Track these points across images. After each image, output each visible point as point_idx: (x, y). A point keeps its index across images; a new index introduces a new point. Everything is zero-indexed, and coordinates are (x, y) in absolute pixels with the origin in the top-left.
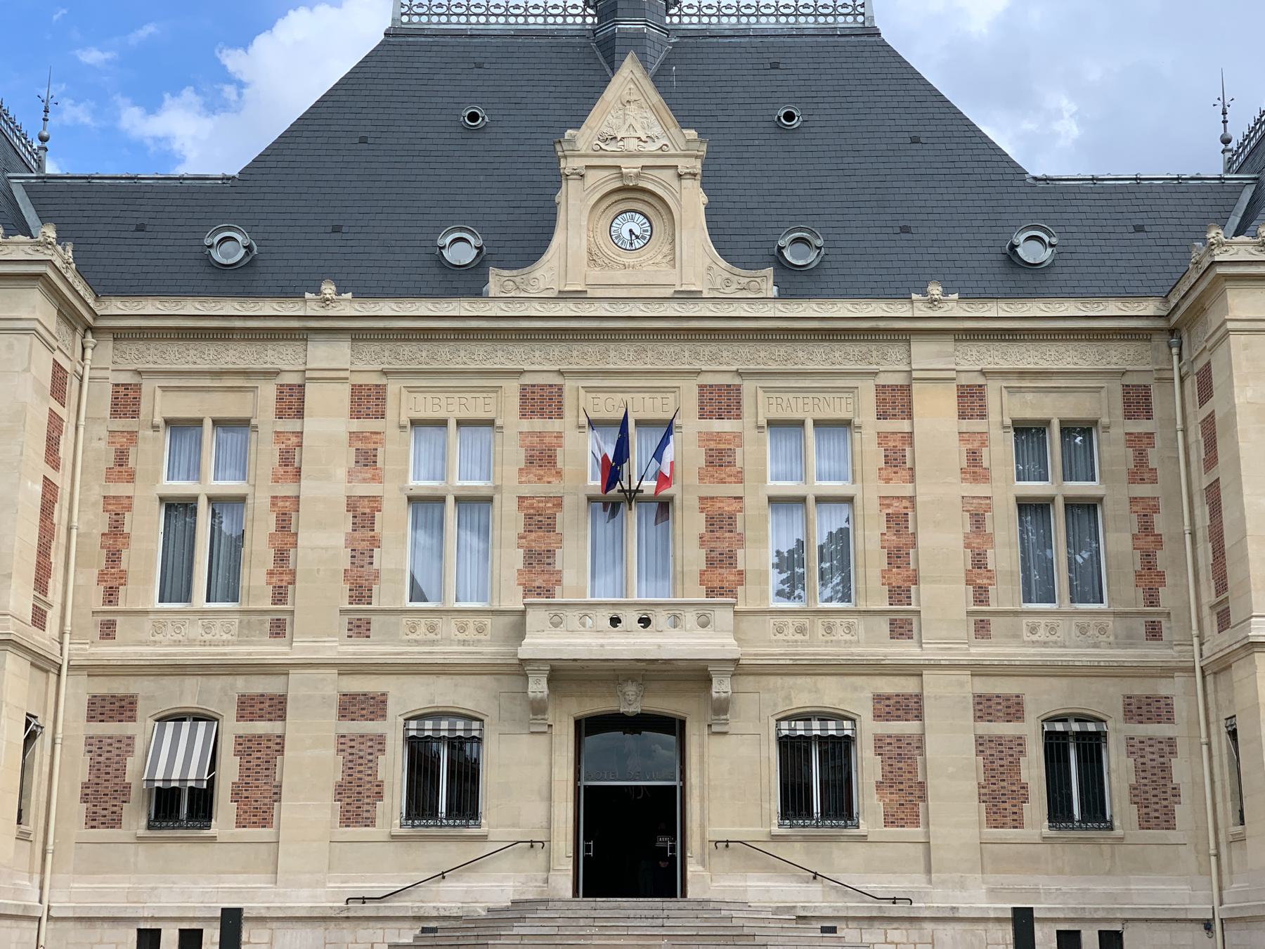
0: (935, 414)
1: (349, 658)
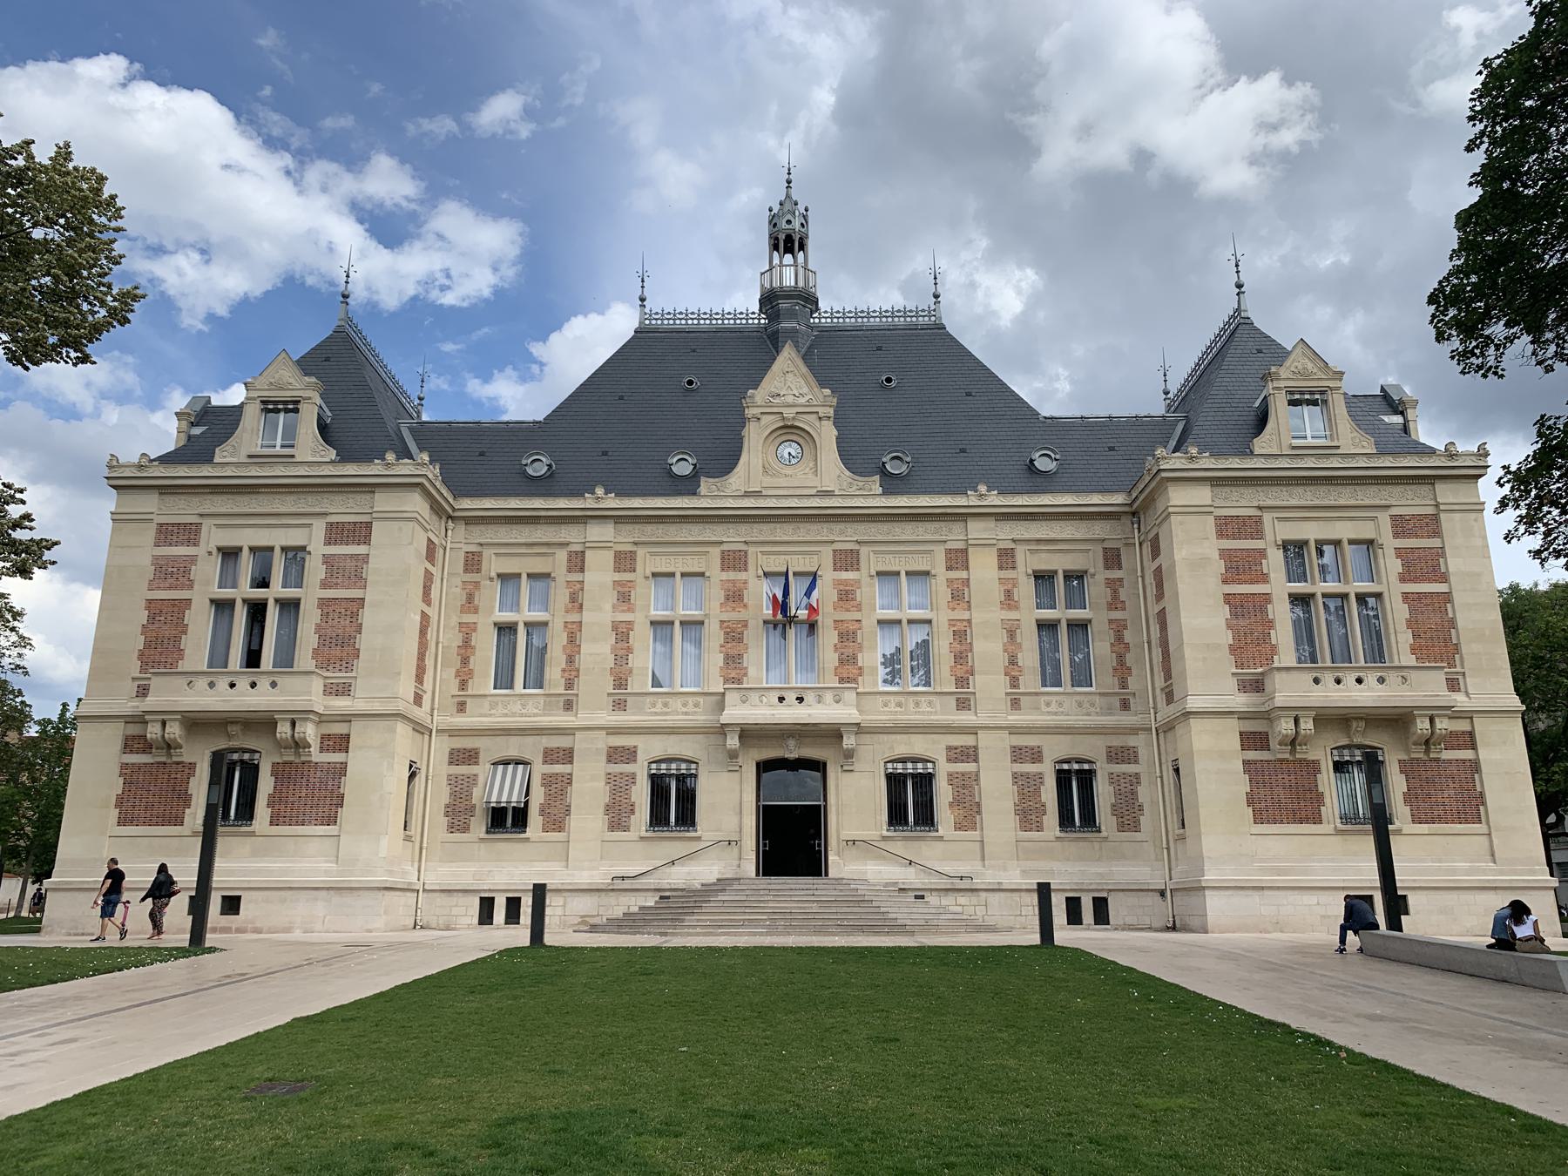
0: (984, 567)
1: (613, 724)
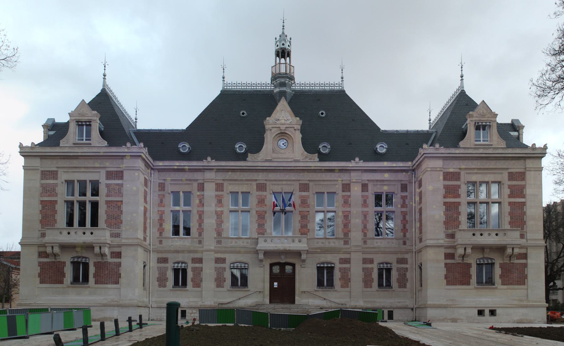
0: (356, 190)
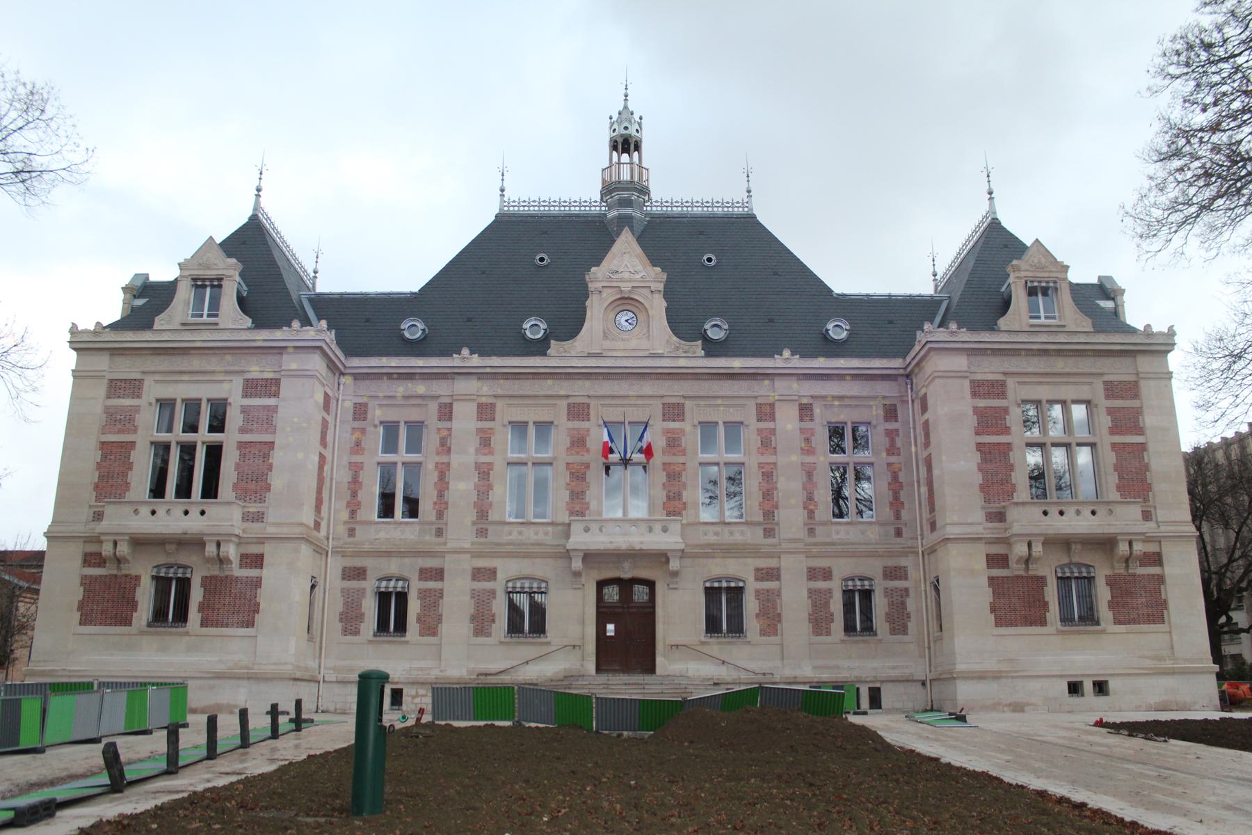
0: (787, 422)
